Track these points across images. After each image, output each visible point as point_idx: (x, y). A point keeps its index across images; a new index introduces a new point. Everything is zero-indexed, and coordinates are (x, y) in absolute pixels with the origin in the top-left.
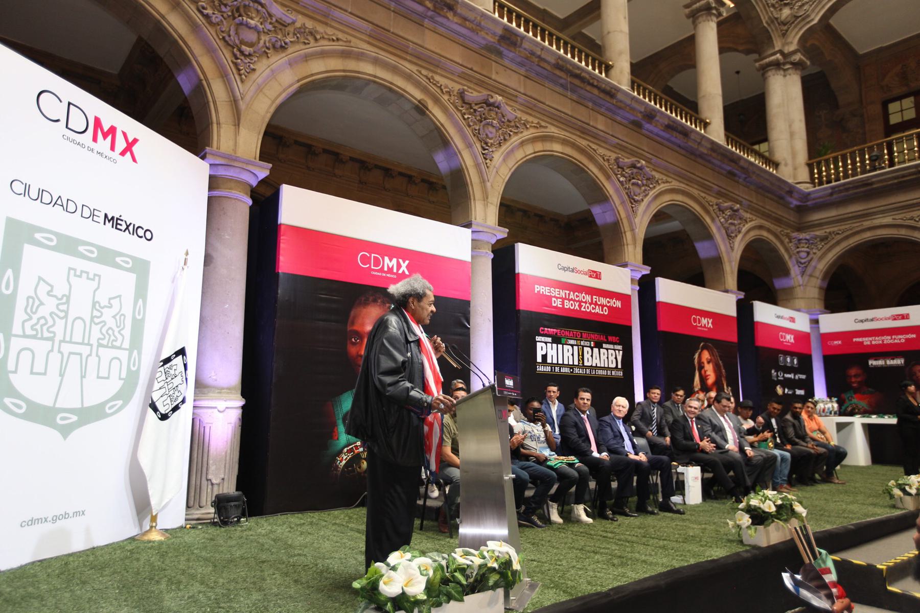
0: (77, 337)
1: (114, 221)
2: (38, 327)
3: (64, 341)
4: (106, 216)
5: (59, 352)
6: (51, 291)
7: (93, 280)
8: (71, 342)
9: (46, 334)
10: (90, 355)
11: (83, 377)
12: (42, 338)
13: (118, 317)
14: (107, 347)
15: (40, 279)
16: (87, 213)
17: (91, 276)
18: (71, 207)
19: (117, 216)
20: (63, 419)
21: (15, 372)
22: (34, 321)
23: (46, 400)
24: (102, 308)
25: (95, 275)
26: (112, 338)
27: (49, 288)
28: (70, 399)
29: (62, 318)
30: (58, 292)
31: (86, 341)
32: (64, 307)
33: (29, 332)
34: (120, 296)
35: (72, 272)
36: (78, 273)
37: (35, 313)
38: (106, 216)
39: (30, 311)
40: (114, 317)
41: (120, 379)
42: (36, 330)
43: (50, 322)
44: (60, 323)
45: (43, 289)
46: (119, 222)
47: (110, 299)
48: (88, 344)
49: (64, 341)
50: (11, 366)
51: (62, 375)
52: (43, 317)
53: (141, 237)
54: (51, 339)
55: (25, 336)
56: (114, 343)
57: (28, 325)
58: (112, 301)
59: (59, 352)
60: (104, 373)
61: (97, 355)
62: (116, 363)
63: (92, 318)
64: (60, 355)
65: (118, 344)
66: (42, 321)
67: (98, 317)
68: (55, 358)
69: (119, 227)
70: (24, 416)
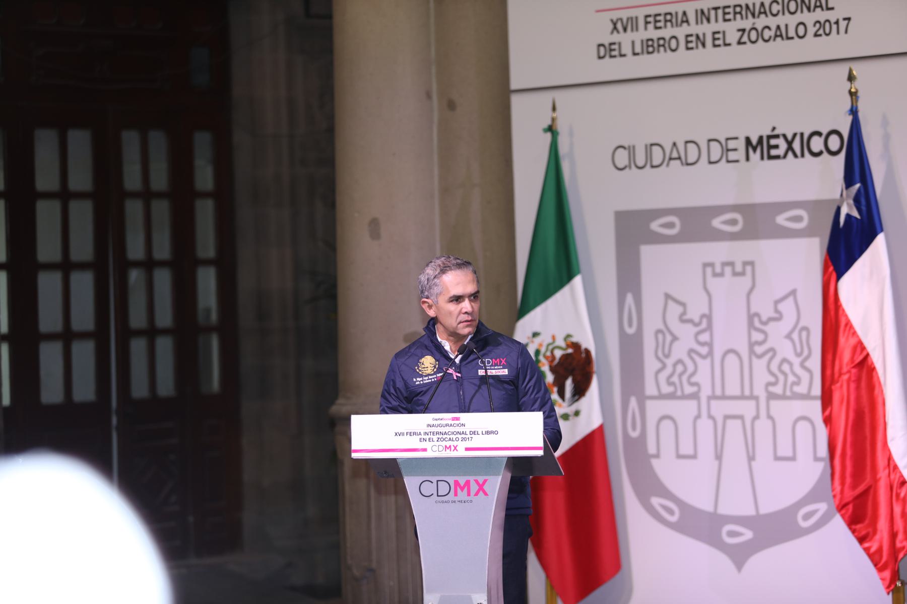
1: (762, 146)
2: (675, 379)
3: (713, 397)
4: (748, 141)
5: (711, 417)
6: (684, 313)
7: (743, 274)
8: (724, 397)
9: (689, 390)
10: (757, 417)
11: (751, 458)
12: (684, 397)
13: (795, 336)
14: (783, 397)
15: (668, 297)
17: (739, 268)
18: (692, 156)
19: (767, 132)
20: (732, 534)
21: (657, 456)
22: (669, 370)
23: (704, 503)
24: (765, 323)
25: (745, 264)
26: (791, 378)
27: (680, 309)
28: (735, 502)
30: (694, 313)
32: (704, 337)
33: (666, 389)
34: (793, 293)
35: (709, 270)
36: (718, 269)
37: (667, 356)
38: (748, 141)
39: (663, 355)
40: (789, 336)
41: (817, 459)
42: (673, 384)
43: (691, 368)
44: (704, 365)
45: (674, 310)
46: (773, 142)
47: (777, 302)
48: (752, 397)
49: (713, 397)
50: (652, 450)
51: (719, 457)
52: (680, 361)
54: (695, 396)
55: (662, 397)
56: (797, 389)
57: (663, 377)
58: (781, 307)
59: (711, 417)
60: (785, 450)
61: (770, 417)
62: (803, 426)
63: (752, 345)
64: (711, 422)
65: (802, 389)
66: (680, 368)
67: (760, 343)
68: (705, 425)
69: (774, 152)
70: (676, 527)
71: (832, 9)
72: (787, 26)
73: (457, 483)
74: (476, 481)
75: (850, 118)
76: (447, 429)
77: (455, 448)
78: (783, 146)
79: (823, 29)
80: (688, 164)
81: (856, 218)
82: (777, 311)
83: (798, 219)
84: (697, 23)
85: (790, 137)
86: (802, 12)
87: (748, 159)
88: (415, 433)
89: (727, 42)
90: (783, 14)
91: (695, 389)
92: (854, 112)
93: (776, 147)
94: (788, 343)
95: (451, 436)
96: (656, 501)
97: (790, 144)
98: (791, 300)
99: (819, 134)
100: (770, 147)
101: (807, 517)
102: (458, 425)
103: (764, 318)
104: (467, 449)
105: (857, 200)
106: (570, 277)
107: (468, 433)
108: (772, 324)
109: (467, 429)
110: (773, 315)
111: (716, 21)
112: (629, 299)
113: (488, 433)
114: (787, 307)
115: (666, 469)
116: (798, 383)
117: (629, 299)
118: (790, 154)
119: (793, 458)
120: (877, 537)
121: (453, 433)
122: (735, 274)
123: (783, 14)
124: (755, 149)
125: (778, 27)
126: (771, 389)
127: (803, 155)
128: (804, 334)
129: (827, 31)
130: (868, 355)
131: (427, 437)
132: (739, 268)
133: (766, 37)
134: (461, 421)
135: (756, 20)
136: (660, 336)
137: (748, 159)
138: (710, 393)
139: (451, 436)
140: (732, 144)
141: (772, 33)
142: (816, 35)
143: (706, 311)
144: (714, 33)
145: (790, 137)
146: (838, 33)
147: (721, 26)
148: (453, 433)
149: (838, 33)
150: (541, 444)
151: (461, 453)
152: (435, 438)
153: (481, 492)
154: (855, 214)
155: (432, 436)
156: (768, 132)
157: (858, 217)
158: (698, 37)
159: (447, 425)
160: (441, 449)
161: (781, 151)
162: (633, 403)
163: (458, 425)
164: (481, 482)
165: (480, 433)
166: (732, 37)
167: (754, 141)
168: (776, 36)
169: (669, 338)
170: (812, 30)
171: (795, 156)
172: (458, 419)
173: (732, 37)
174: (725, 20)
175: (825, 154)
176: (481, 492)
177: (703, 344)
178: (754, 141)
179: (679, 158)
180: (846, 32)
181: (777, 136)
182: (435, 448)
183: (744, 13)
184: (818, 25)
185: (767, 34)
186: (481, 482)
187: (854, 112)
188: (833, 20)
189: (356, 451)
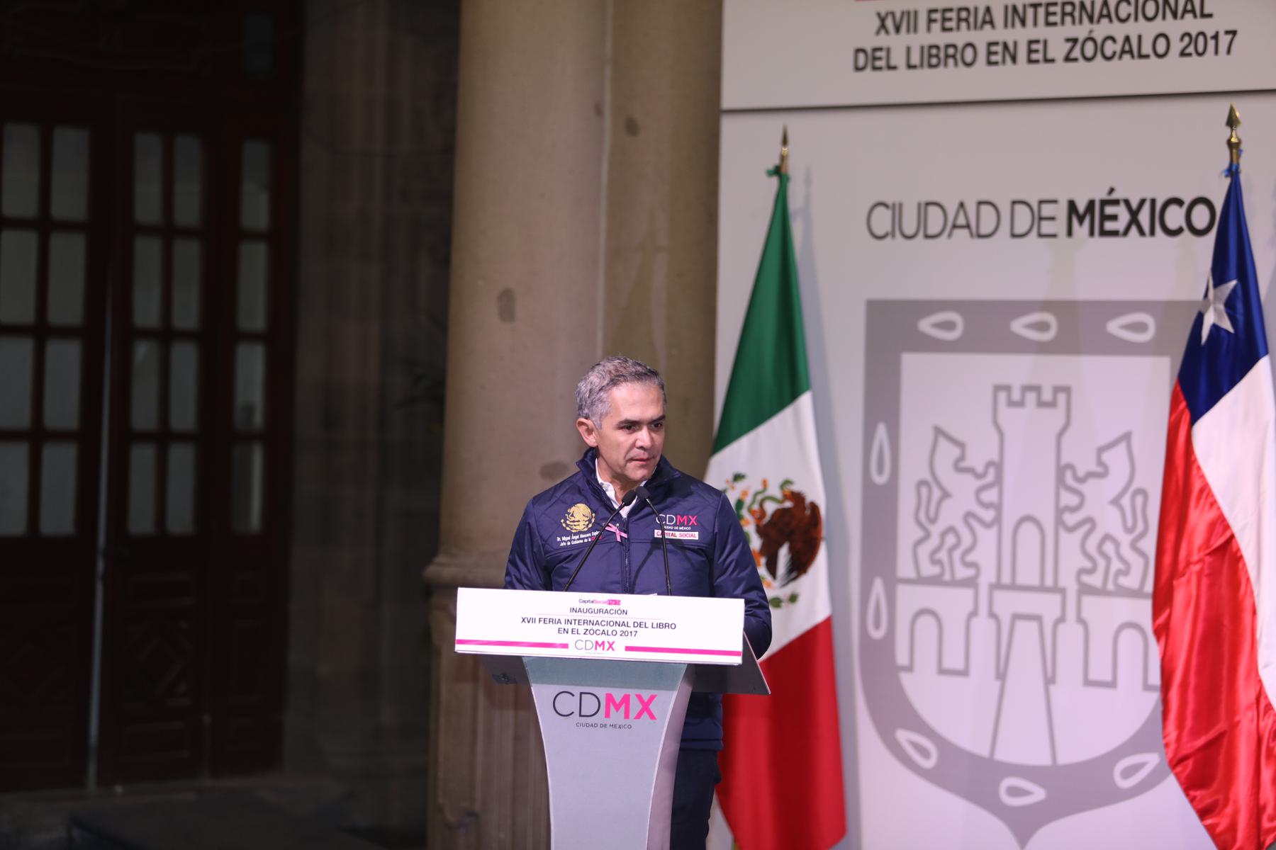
0: (1029, 575)
1: (1093, 216)
2: (943, 555)
3: (997, 586)
4: (1072, 206)
5: (992, 615)
6: (962, 458)
7: (1052, 404)
8: (1014, 587)
9: (962, 572)
10: (1061, 619)
11: (1050, 680)
12: (955, 583)
13: (1126, 501)
14: (1102, 592)
15: (939, 432)
16: (1023, 219)
17: (1047, 396)
19: (1101, 194)
20: (1014, 792)
24: (1082, 480)
25: (1057, 390)
26: (1116, 565)
28: (1022, 745)
29: (987, 525)
30: (976, 459)
31: (1049, 582)
32: (990, 496)
33: (929, 570)
34: (1127, 437)
35: (1002, 396)
36: (1016, 396)
37: (933, 521)
38: (1072, 206)
40: (1116, 502)
41: (1147, 687)
43: (967, 540)
44: (987, 537)
45: (947, 452)
46: (1109, 210)
47: (1101, 450)
49: (997, 586)
50: (902, 658)
51: (1001, 676)
52: (951, 529)
53: (1178, 231)
54: (971, 583)
55: (921, 580)
56: (1123, 581)
57: (924, 551)
58: (1106, 457)
59: (992, 615)
60: (1100, 671)
61: (1081, 620)
63: (1060, 512)
64: (992, 624)
65: (1131, 581)
66: (951, 540)
68: (983, 627)
69: (1109, 226)
70: (931, 776)
71: (1210, 16)
72: (1140, 37)
73: (610, 698)
74: (639, 697)
75: (1227, 182)
76: (600, 617)
77: (611, 646)
78: (1124, 217)
79: (1194, 45)
80: (980, 236)
81: (1228, 332)
82: (1100, 463)
83: (1140, 327)
84: (1006, 25)
85: (1134, 205)
86: (1164, 17)
87: (1070, 233)
88: (551, 621)
89: (1050, 56)
90: (1136, 19)
91: (970, 572)
92: (1233, 172)
93: (1114, 218)
94: (1114, 512)
95: (606, 628)
96: (903, 736)
97: (1134, 214)
98: (1122, 447)
99: (1179, 202)
100: (1104, 218)
101: (1128, 773)
102: (616, 612)
103: (1081, 473)
104: (628, 649)
105: (1230, 305)
106: (794, 394)
107: (631, 624)
108: (1092, 482)
109: (629, 618)
110: (1094, 468)
111: (1035, 24)
112: (881, 432)
113: (660, 626)
114: (1117, 459)
115: (923, 690)
116: (1126, 572)
117: (881, 432)
118: (1134, 230)
119: (1112, 684)
120: (1229, 810)
121: (608, 623)
122: (1041, 404)
123: (1136, 19)
124: (1081, 220)
125: (1127, 39)
126: (1086, 579)
127: (1152, 233)
128: (1139, 499)
129: (1200, 49)
130: (1232, 536)
131: (569, 627)
132: (1047, 396)
133: (1108, 53)
134: (622, 607)
135: (1095, 27)
136: (924, 490)
137: (1070, 233)
138: (993, 579)
139: (606, 628)
140: (1047, 210)
141: (1118, 48)
142: (1183, 54)
143: (995, 458)
144: (1031, 42)
145: (1134, 205)
146: (1216, 52)
147: (1041, 32)
148: (608, 623)
149: (1216, 52)
150: (740, 648)
151: (619, 654)
152: (582, 629)
153: (645, 715)
154: (1227, 325)
155: (577, 626)
156: (1104, 196)
157: (1231, 330)
158: (1006, 46)
159: (600, 611)
160: (589, 645)
161: (1120, 225)
162: (878, 586)
163: (616, 612)
164: (646, 698)
165: (649, 625)
166: (1058, 49)
167: (1081, 207)
168: (1123, 52)
169: (937, 494)
170: (1177, 46)
171: (1142, 233)
172: (617, 602)
173: (1058, 49)
174: (1048, 24)
175: (1187, 233)
176: (645, 715)
177: (987, 506)
178: (1081, 207)
179: (968, 226)
180: (1229, 52)
181: (1116, 202)
182: (580, 645)
183: (1077, 14)
184: (1187, 39)
185: (1110, 48)
186: (646, 698)
187: (1233, 172)
188: (1210, 33)
189: (461, 642)
